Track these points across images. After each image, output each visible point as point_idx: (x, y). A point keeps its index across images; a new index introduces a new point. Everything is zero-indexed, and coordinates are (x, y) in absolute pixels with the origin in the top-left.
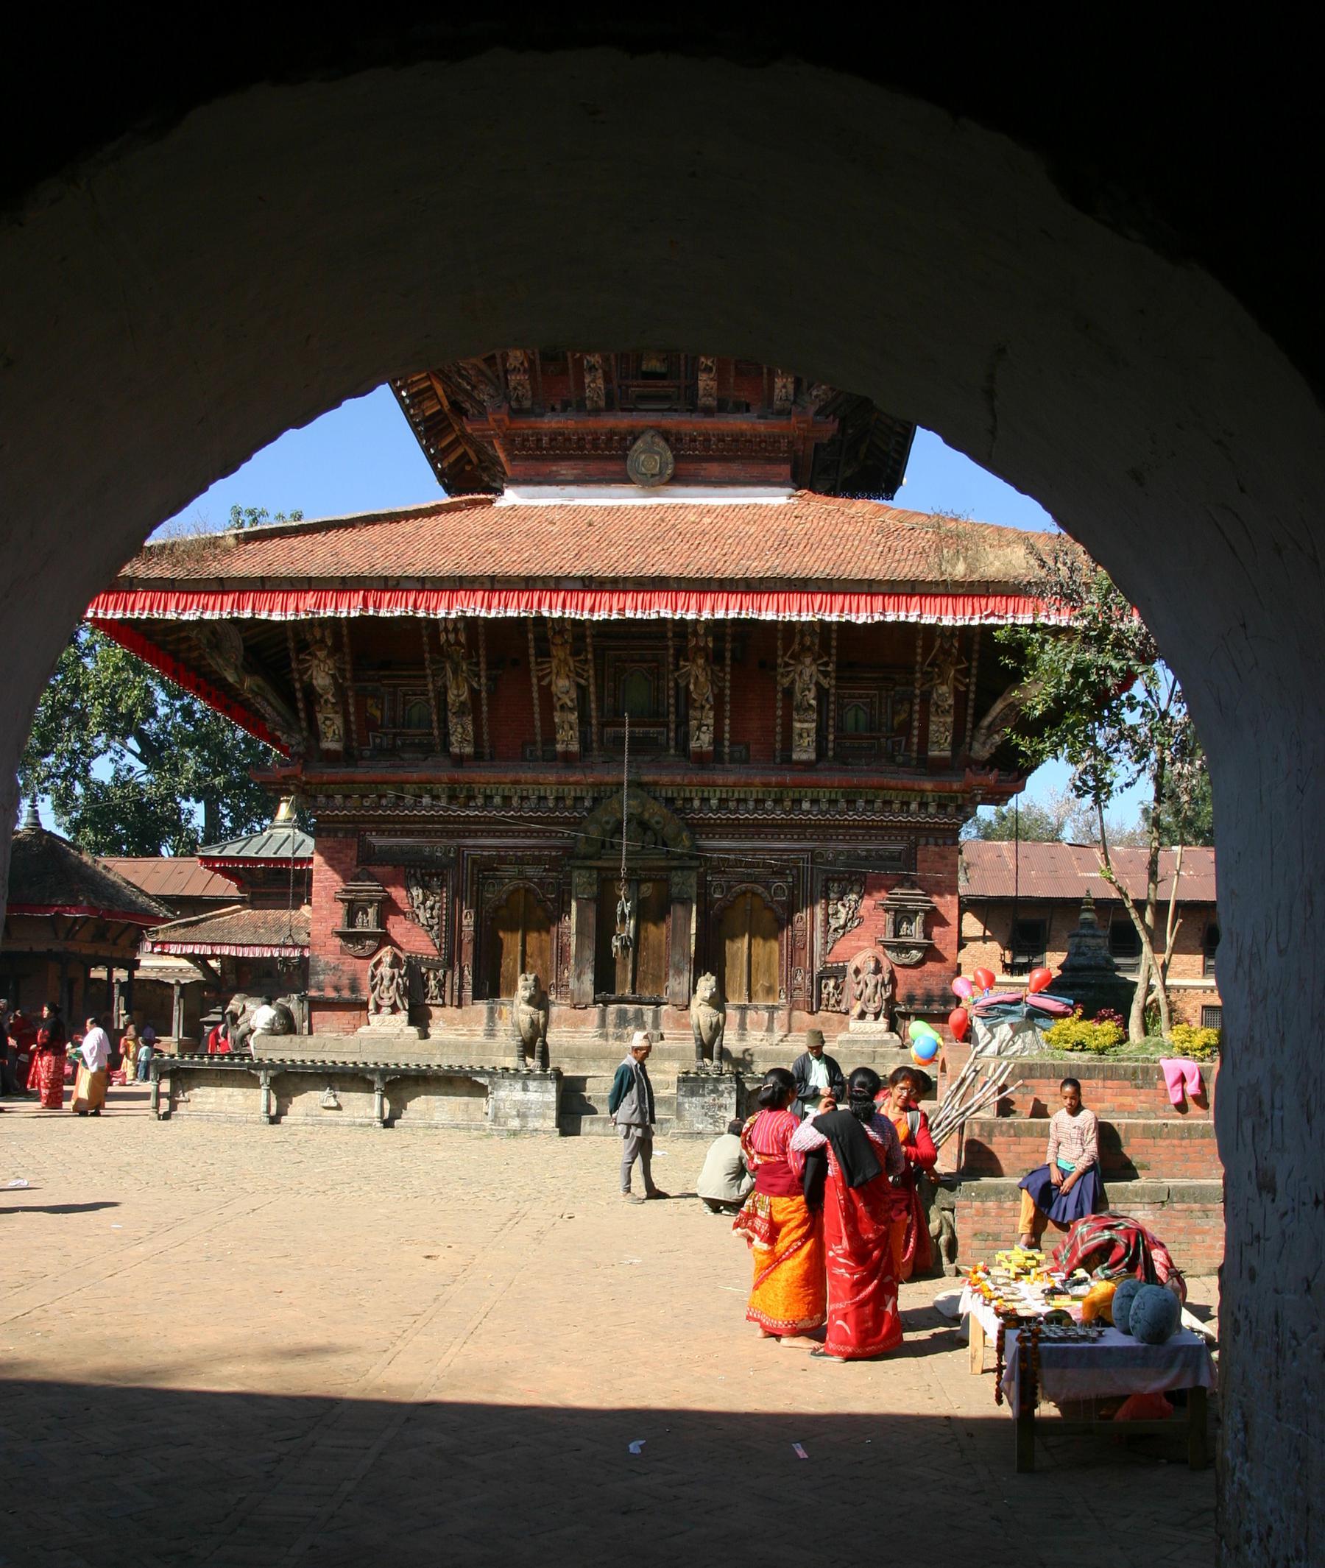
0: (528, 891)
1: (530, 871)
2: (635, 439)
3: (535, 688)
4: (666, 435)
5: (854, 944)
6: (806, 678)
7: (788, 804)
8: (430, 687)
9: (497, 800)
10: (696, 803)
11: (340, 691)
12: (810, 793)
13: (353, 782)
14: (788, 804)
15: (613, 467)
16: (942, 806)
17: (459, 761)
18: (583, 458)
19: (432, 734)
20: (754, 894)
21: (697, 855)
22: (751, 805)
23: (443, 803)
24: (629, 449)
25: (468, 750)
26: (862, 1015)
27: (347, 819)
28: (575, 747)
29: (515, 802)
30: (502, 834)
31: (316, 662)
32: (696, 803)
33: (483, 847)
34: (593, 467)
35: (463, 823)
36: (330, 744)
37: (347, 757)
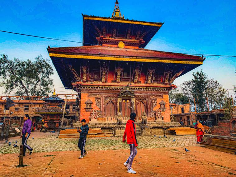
3: (115, 73)
6: (151, 72)
7: (147, 89)
8: (100, 72)
9: (108, 88)
10: (135, 89)
11: (87, 72)
12: (150, 88)
13: (88, 85)
15: (116, 46)
16: (167, 90)
17: (103, 82)
18: (112, 44)
19: (99, 79)
22: (142, 89)
23: (101, 88)
25: (104, 81)
26: (158, 117)
28: (119, 81)
29: (111, 88)
32: (135, 89)
34: (114, 46)
36: (83, 80)
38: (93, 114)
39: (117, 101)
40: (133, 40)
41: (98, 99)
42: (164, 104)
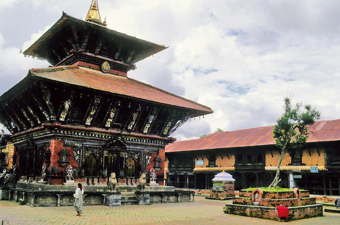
0: (93, 154)
1: (95, 150)
2: (103, 62)
4: (109, 62)
5: (150, 167)
14: (142, 140)
15: (97, 67)
17: (87, 126)
20: (133, 157)
21: (126, 148)
24: (102, 64)
27: (61, 136)
28: (109, 126)
30: (92, 142)
31: (67, 102)
33: (87, 145)
35: (85, 139)
37: (63, 123)
38: (70, 173)
39: (101, 155)
40: (122, 63)
41: (77, 150)
42: (160, 161)
